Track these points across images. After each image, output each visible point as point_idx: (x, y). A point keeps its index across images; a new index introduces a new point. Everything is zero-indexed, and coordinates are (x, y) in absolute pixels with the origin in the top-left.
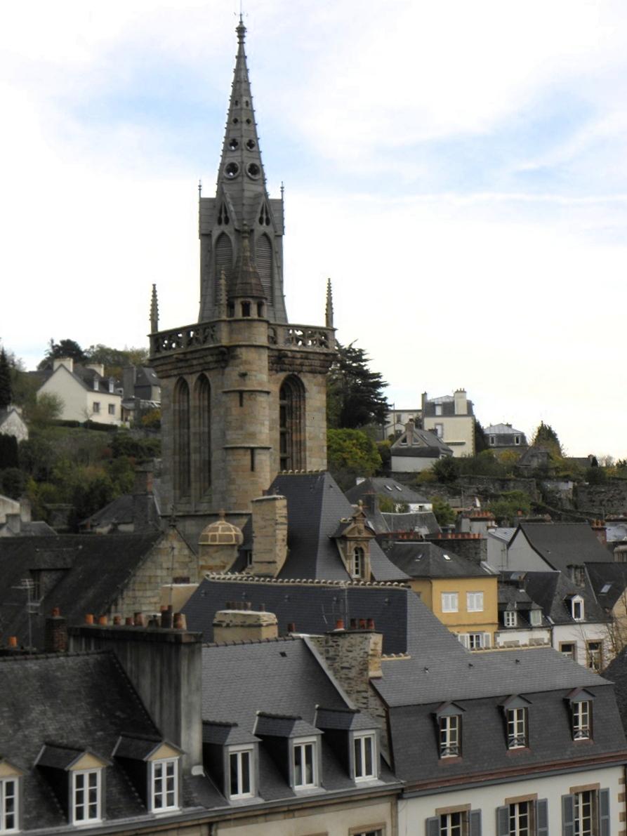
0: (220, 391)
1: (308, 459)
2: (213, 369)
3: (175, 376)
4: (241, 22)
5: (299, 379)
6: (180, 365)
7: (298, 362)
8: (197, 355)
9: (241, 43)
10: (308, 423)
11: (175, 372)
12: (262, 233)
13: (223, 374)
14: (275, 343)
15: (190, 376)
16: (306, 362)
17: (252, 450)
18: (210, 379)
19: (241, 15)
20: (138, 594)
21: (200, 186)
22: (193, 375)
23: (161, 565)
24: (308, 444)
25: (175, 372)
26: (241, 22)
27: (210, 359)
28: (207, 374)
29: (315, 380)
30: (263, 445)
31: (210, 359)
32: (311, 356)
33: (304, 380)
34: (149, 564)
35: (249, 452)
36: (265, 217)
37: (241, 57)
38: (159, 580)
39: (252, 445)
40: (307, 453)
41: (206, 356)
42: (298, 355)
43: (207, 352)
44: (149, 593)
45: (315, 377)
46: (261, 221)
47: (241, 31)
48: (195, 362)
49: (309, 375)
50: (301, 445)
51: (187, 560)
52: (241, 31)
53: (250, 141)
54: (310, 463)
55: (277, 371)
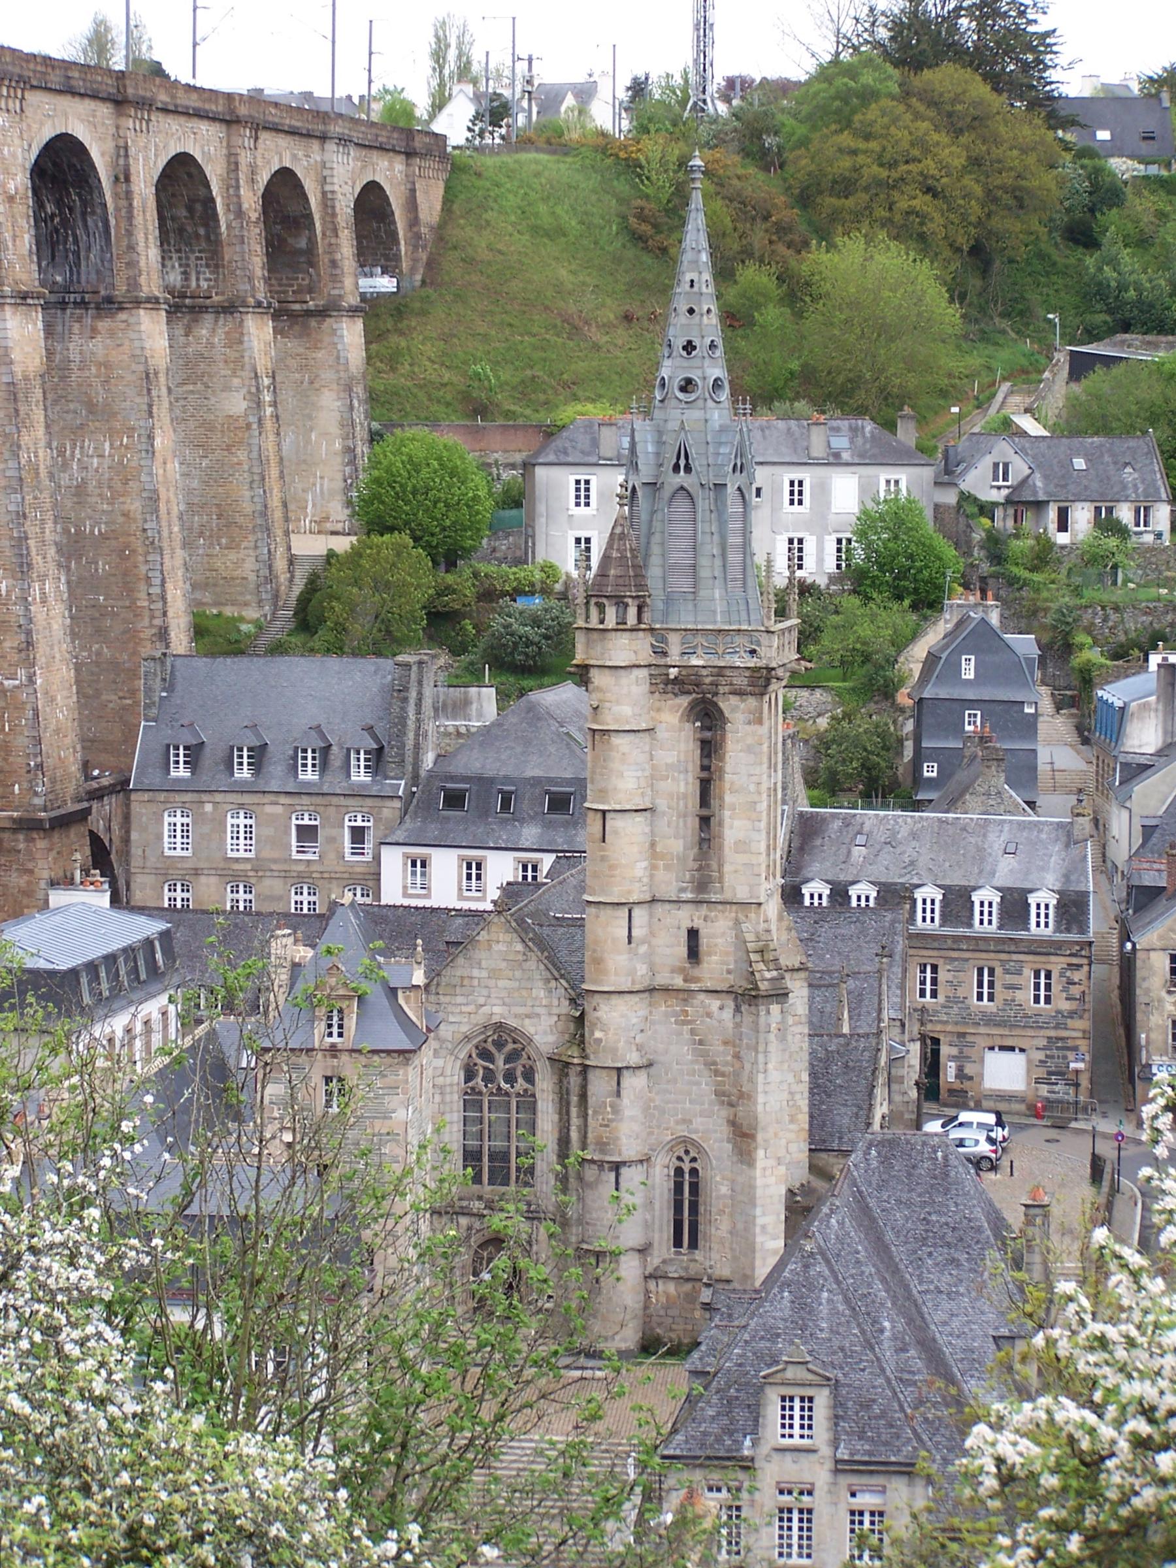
1: (727, 821)
5: (716, 704)
7: (708, 680)
10: (728, 768)
12: (677, 486)
14: (665, 654)
16: (722, 680)
17: (604, 812)
20: (442, 999)
23: (479, 963)
24: (728, 798)
29: (742, 706)
30: (618, 807)
32: (728, 672)
33: (721, 704)
34: (461, 961)
35: (599, 815)
36: (682, 463)
38: (476, 982)
39: (601, 807)
40: (727, 813)
42: (704, 672)
44: (459, 1000)
45: (743, 701)
46: (676, 468)
49: (734, 700)
50: (721, 798)
51: (521, 957)
53: (690, 342)
54: (731, 827)
55: (676, 695)
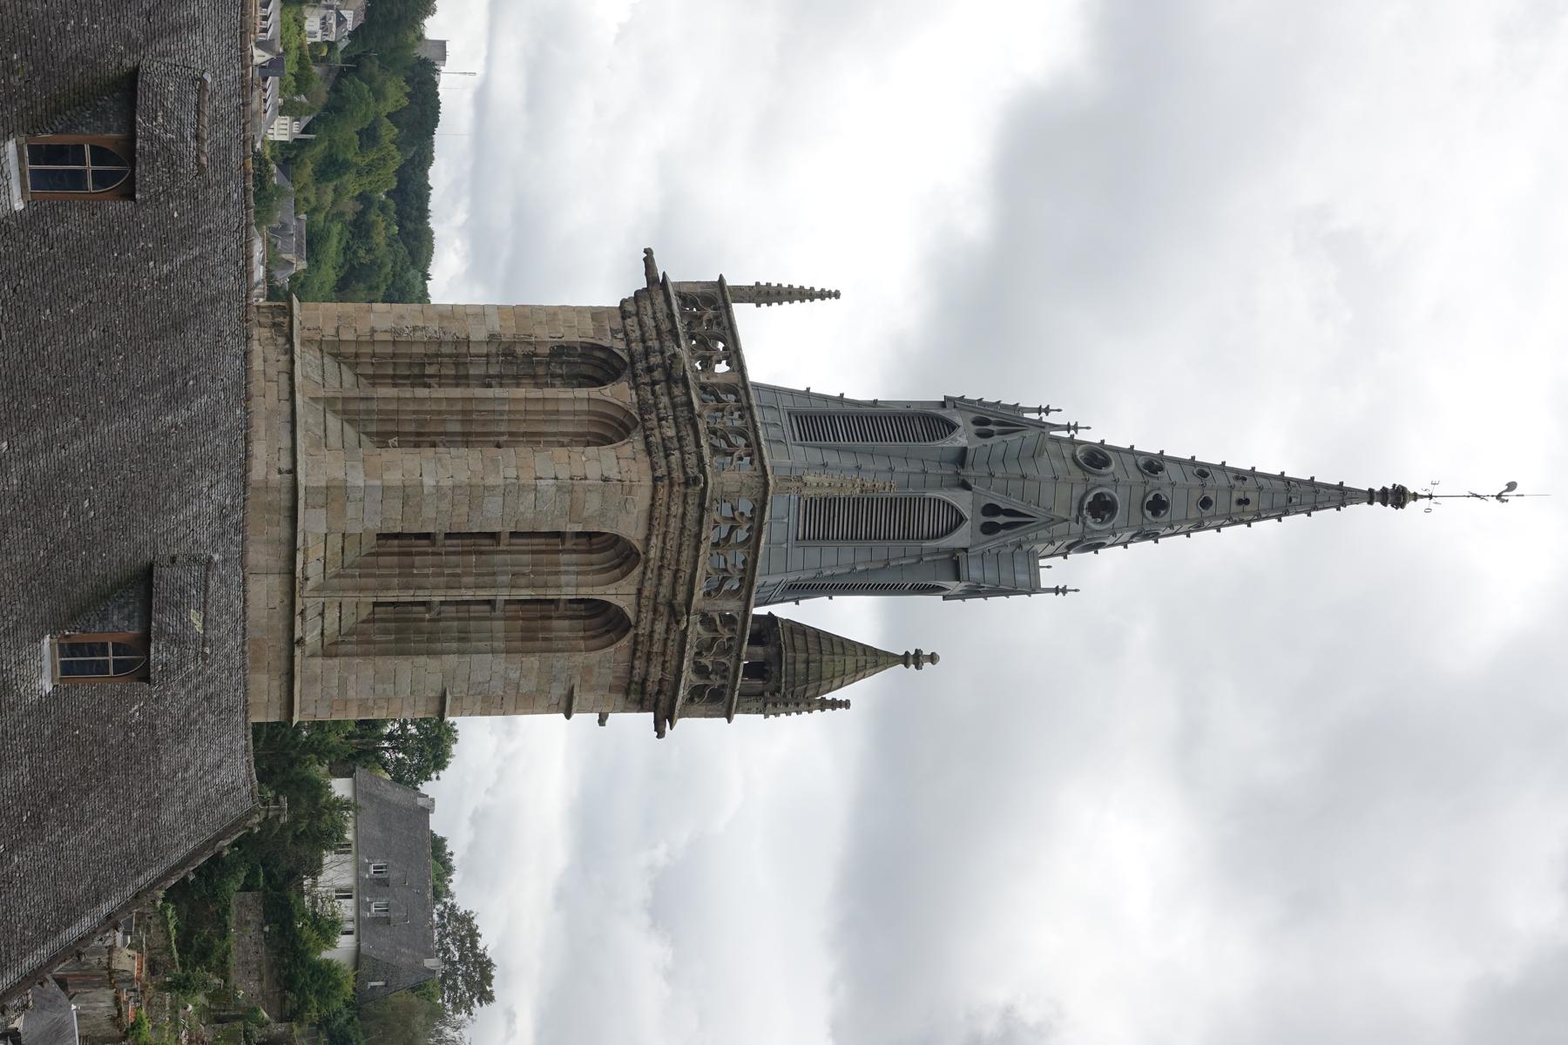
0: (577, 681)
2: (632, 667)
3: (648, 539)
4: (1415, 497)
6: (668, 575)
8: (672, 648)
9: (1371, 496)
11: (654, 553)
13: (611, 689)
15: (633, 590)
18: (611, 649)
19: (1431, 497)
21: (1064, 591)
22: (633, 599)
25: (654, 553)
26: (1415, 497)
27: (656, 672)
28: (625, 642)
31: (656, 672)
37: (1341, 496)
41: (663, 670)
43: (670, 677)
47: (1397, 497)
48: (660, 627)
52: (1397, 497)
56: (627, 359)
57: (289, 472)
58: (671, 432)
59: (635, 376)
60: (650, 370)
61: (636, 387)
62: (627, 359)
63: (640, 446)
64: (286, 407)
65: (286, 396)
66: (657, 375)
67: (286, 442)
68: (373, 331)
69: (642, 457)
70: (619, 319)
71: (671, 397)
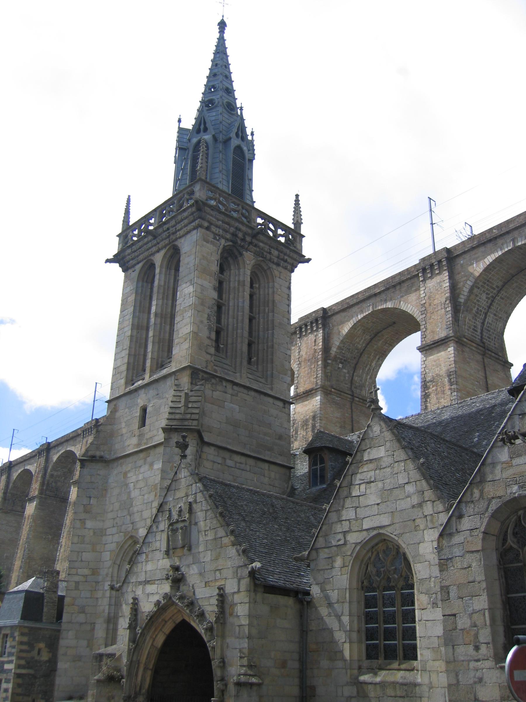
4: (223, 19)
26: (223, 19)
47: (222, 25)
52: (222, 25)
56: (231, 243)
57: (284, 404)
58: (276, 253)
59: (243, 247)
60: (243, 240)
61: (247, 250)
62: (231, 243)
63: (274, 267)
64: (252, 393)
65: (245, 391)
66: (248, 239)
67: (271, 400)
68: (209, 338)
69: (280, 269)
70: (208, 232)
71: (262, 242)
